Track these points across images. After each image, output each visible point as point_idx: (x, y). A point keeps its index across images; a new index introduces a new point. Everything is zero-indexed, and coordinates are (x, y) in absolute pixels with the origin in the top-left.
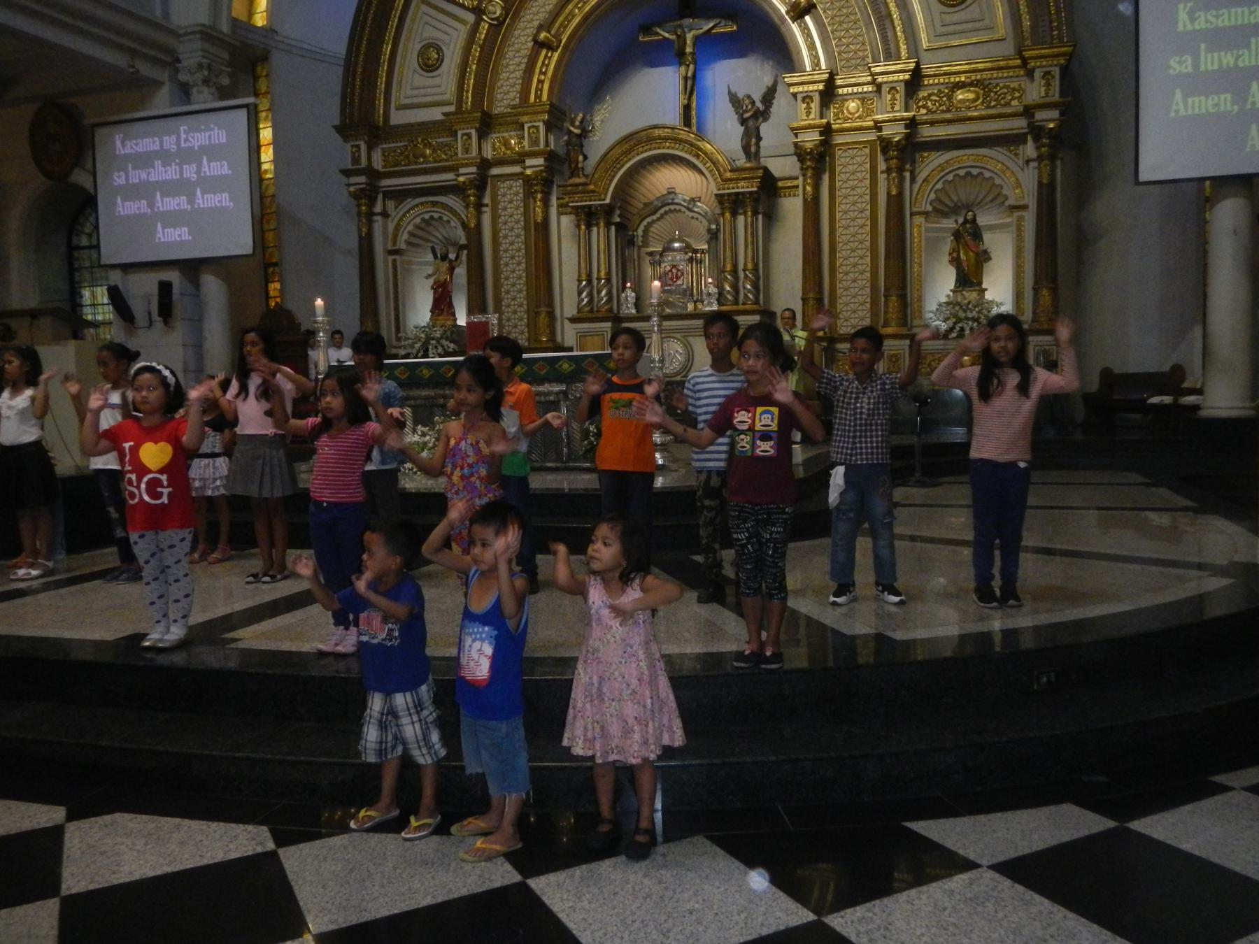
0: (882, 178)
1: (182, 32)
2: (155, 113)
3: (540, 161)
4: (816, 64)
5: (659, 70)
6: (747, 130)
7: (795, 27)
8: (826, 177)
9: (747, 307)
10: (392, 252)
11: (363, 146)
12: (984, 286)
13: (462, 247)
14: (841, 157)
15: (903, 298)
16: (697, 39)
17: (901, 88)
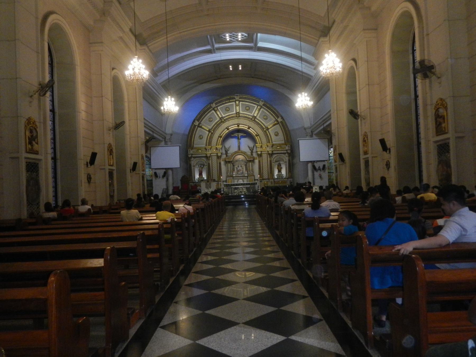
0: (269, 158)
2: (161, 146)
3: (220, 154)
7: (256, 137)
8: (261, 158)
9: (252, 175)
10: (193, 166)
13: (204, 165)
14: (263, 155)
15: (272, 174)
17: (271, 147)
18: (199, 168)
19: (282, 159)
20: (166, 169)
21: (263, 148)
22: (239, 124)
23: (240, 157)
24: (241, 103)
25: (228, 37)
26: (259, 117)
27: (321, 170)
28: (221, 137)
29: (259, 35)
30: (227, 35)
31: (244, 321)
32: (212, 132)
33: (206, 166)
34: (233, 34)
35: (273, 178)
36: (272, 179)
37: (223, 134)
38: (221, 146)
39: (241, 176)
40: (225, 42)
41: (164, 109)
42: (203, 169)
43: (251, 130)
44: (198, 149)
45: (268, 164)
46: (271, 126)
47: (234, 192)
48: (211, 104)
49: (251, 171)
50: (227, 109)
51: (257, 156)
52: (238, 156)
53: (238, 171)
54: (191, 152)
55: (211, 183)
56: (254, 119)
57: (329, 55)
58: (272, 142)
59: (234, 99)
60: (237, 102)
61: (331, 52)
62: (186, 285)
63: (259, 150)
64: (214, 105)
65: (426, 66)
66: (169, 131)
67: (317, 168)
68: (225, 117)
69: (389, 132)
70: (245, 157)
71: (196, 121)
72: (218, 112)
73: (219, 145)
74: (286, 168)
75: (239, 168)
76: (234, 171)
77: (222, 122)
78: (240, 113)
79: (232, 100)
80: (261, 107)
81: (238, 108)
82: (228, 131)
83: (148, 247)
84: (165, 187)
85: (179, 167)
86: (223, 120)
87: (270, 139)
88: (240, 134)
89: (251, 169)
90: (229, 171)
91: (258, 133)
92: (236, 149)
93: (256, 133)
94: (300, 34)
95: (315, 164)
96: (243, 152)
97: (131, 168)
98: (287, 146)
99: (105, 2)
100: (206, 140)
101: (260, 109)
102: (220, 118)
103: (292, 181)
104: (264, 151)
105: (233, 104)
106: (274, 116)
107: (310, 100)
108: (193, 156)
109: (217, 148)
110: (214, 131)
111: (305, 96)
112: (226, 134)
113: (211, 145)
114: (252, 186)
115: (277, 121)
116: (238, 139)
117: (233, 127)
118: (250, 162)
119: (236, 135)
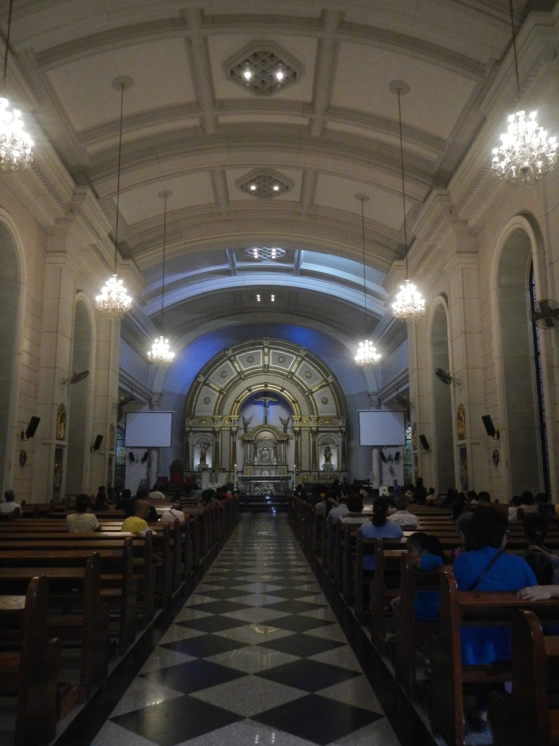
1: (155, 393)
4: (297, 413)
5: (256, 406)
6: (284, 427)
7: (293, 405)
8: (299, 437)
9: (284, 464)
11: (190, 420)
12: (331, 461)
13: (209, 445)
14: (303, 433)
15: (316, 463)
16: (268, 402)
17: (315, 420)
18: (200, 449)
19: (332, 440)
20: (148, 448)
21: (303, 423)
22: (268, 383)
23: (267, 435)
24: (272, 352)
25: (256, 254)
26: (299, 374)
27: (392, 461)
28: (238, 402)
29: (303, 252)
30: (255, 250)
31: (252, 714)
32: (226, 393)
33: (212, 446)
34: (265, 249)
35: (319, 470)
36: (314, 472)
37: (241, 398)
38: (238, 416)
39: (267, 464)
40: (253, 260)
41: (152, 355)
42: (207, 451)
43: (285, 394)
44: (201, 419)
45: (309, 445)
46: (317, 388)
47: (254, 491)
48: (226, 351)
49: (282, 457)
50: (250, 359)
51: (293, 434)
52: (263, 432)
53: (262, 457)
54: (191, 423)
55: (218, 474)
56: (290, 376)
57: (405, 287)
58: (317, 414)
59: (261, 345)
60: (266, 350)
61: (409, 282)
62: (164, 646)
63: (297, 424)
64: (230, 353)
65: (550, 309)
66: (157, 388)
67: (387, 456)
68: (246, 371)
69: (496, 405)
70: (275, 435)
71: (200, 375)
72: (236, 363)
73: (234, 414)
74: (338, 455)
75: (264, 452)
76: (257, 456)
77: (241, 379)
78: (269, 366)
79: (259, 347)
80: (303, 359)
81: (266, 358)
82: (249, 393)
83: (104, 577)
84: (145, 477)
85: (170, 445)
86: (243, 376)
87: (314, 408)
88: (269, 399)
89: (282, 455)
90: (248, 457)
91: (295, 399)
92: (260, 421)
93: (294, 398)
94: (364, 253)
95: (384, 451)
96: (271, 427)
97: (93, 445)
98: (340, 420)
99: (74, 194)
100: (214, 405)
101: (301, 361)
102: (239, 373)
103: (347, 477)
104: (304, 426)
105: (260, 352)
106: (322, 372)
107: (377, 353)
108: (193, 429)
109: (232, 418)
110: (227, 393)
111: (370, 346)
112: (246, 397)
113: (222, 415)
114: (283, 481)
115: (326, 380)
116: (265, 406)
117: (257, 388)
118: (281, 444)
119: (262, 399)
